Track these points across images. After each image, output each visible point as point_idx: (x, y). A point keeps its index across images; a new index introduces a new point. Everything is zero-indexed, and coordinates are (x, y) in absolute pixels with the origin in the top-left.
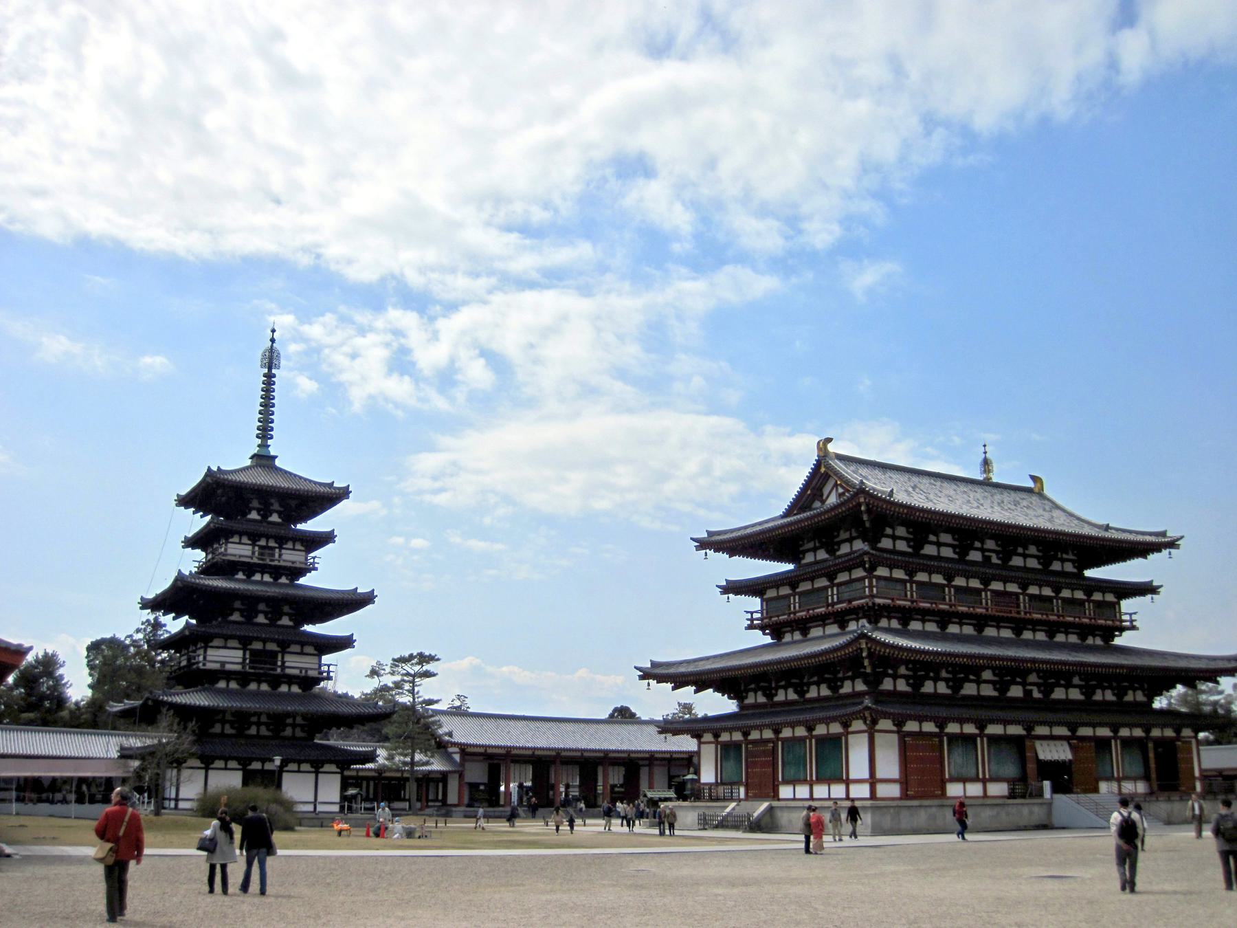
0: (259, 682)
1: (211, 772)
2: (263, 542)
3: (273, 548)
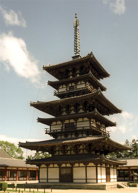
0: (71, 135)
1: (49, 169)
2: (70, 85)
3: (74, 86)
